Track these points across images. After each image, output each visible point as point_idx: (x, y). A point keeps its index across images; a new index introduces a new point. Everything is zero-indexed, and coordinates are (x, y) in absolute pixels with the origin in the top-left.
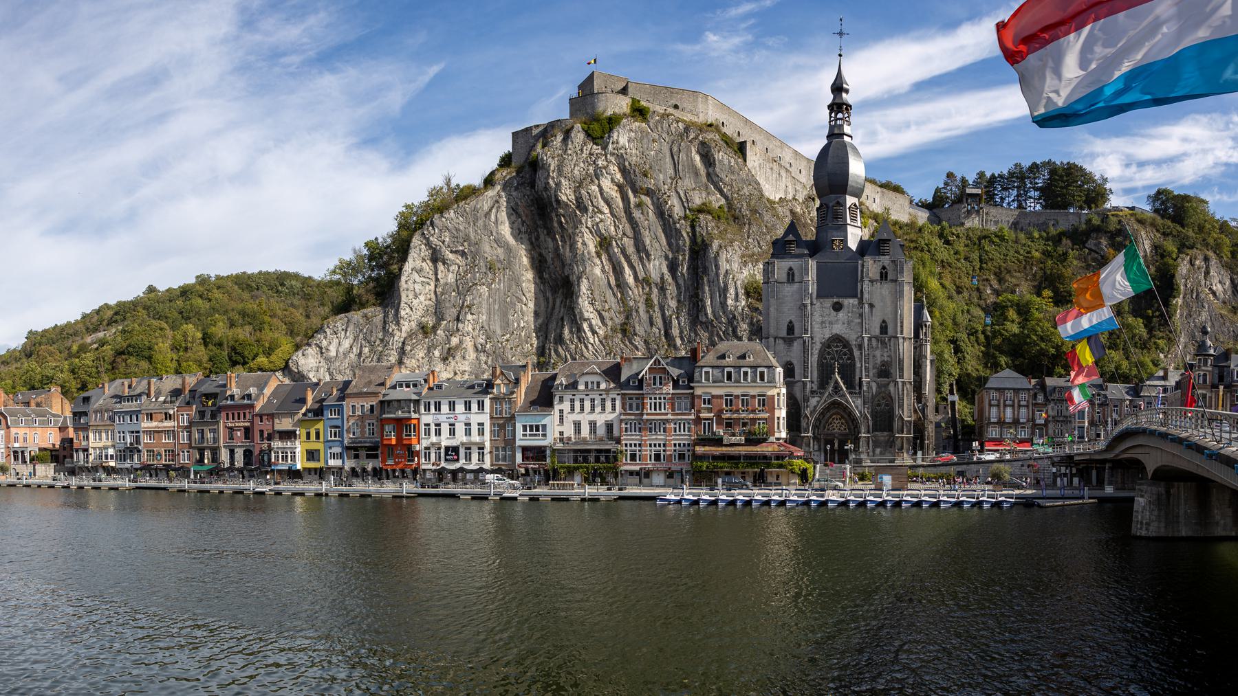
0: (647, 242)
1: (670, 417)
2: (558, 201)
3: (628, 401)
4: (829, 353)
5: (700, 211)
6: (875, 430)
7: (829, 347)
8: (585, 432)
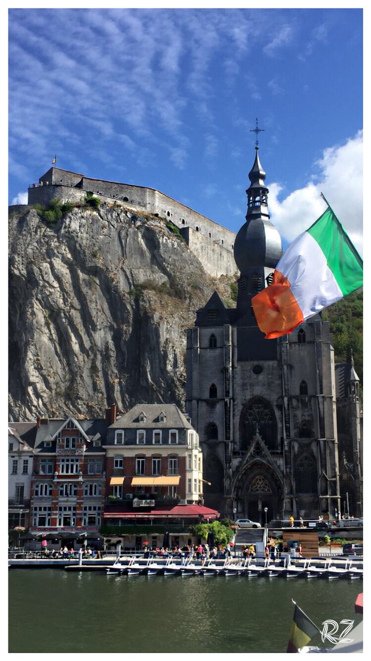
0: (94, 313)
1: (81, 479)
3: (41, 464)
4: (251, 414)
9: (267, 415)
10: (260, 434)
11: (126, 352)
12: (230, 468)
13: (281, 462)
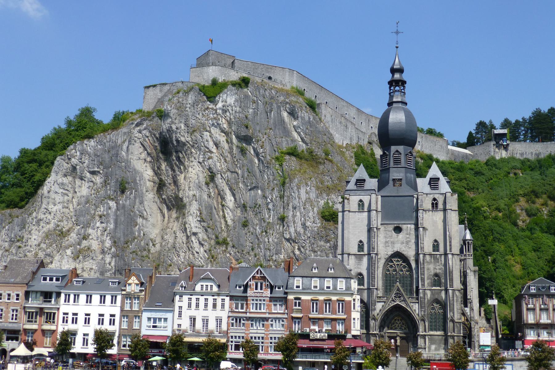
1: (267, 315)
2: (178, 141)
4: (391, 266)
8: (199, 325)
9: (404, 267)
10: (400, 283)
13: (416, 307)
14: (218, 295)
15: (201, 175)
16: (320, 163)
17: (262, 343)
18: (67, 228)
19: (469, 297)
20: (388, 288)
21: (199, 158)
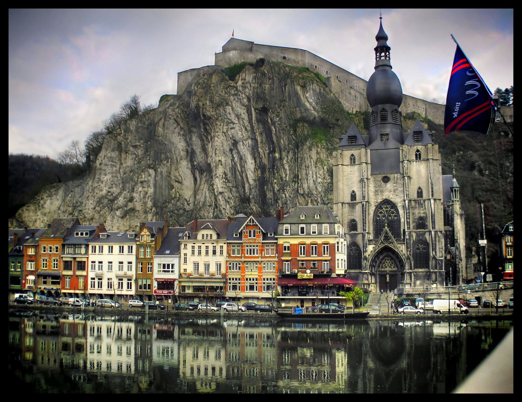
1: (260, 259)
2: (204, 115)
4: (381, 213)
5: (297, 121)
6: (416, 267)
7: (381, 208)
8: (202, 269)
9: (393, 213)
11: (288, 169)
12: (366, 251)
14: (217, 242)
15: (225, 143)
16: (330, 128)
17: (256, 283)
18: (116, 193)
19: (456, 238)
20: (378, 231)
21: (223, 129)
